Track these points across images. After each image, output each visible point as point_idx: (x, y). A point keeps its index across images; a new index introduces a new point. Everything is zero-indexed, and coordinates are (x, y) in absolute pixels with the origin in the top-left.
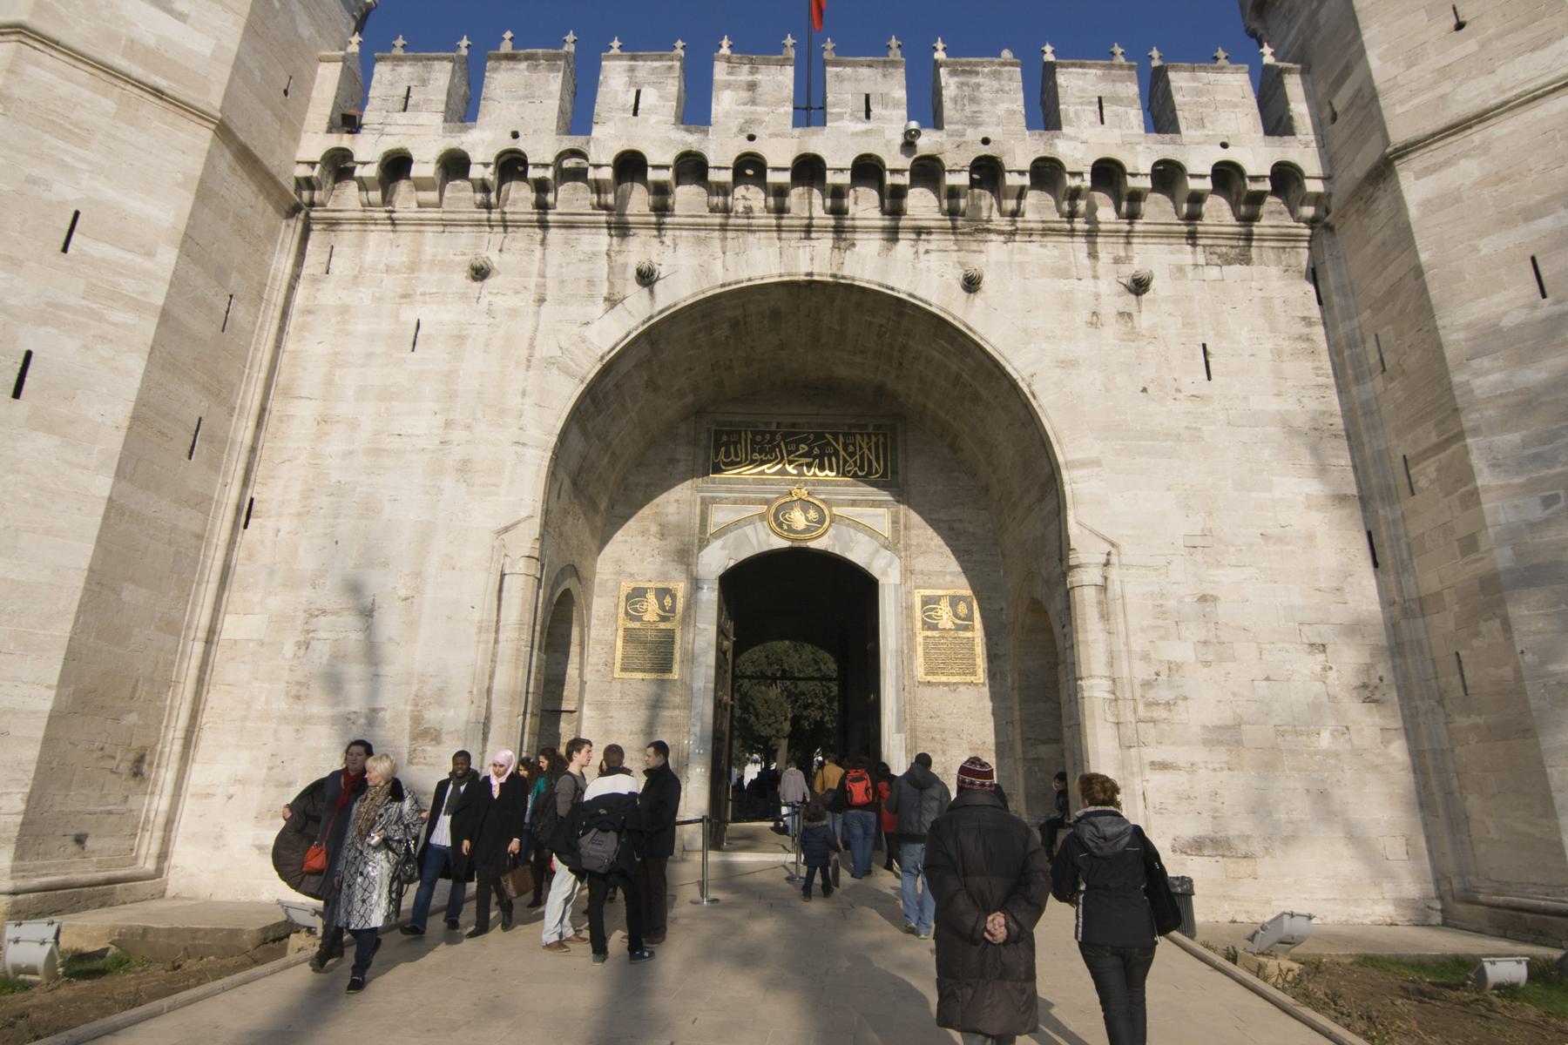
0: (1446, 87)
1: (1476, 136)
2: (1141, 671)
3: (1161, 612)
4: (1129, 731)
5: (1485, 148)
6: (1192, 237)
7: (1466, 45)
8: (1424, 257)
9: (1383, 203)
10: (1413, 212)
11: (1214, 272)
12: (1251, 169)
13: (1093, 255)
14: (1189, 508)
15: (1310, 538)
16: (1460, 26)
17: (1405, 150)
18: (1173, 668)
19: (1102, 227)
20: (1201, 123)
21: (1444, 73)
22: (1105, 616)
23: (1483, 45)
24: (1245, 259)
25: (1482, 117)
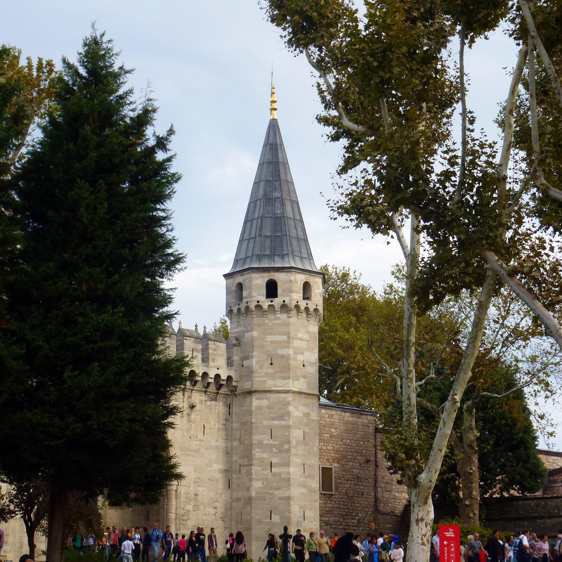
0: (266, 379)
1: (268, 395)
2: (182, 512)
3: (187, 498)
4: (178, 526)
5: (268, 399)
6: (206, 392)
7: (271, 371)
8: (253, 420)
9: (248, 399)
10: (254, 408)
11: (209, 403)
12: (223, 378)
13: (184, 395)
14: (195, 471)
15: (218, 480)
16: (272, 364)
17: (255, 392)
18: (188, 511)
19: (187, 387)
20: (214, 361)
21: (267, 375)
22: (176, 498)
23: (275, 372)
24: (216, 400)
25: (270, 392)
